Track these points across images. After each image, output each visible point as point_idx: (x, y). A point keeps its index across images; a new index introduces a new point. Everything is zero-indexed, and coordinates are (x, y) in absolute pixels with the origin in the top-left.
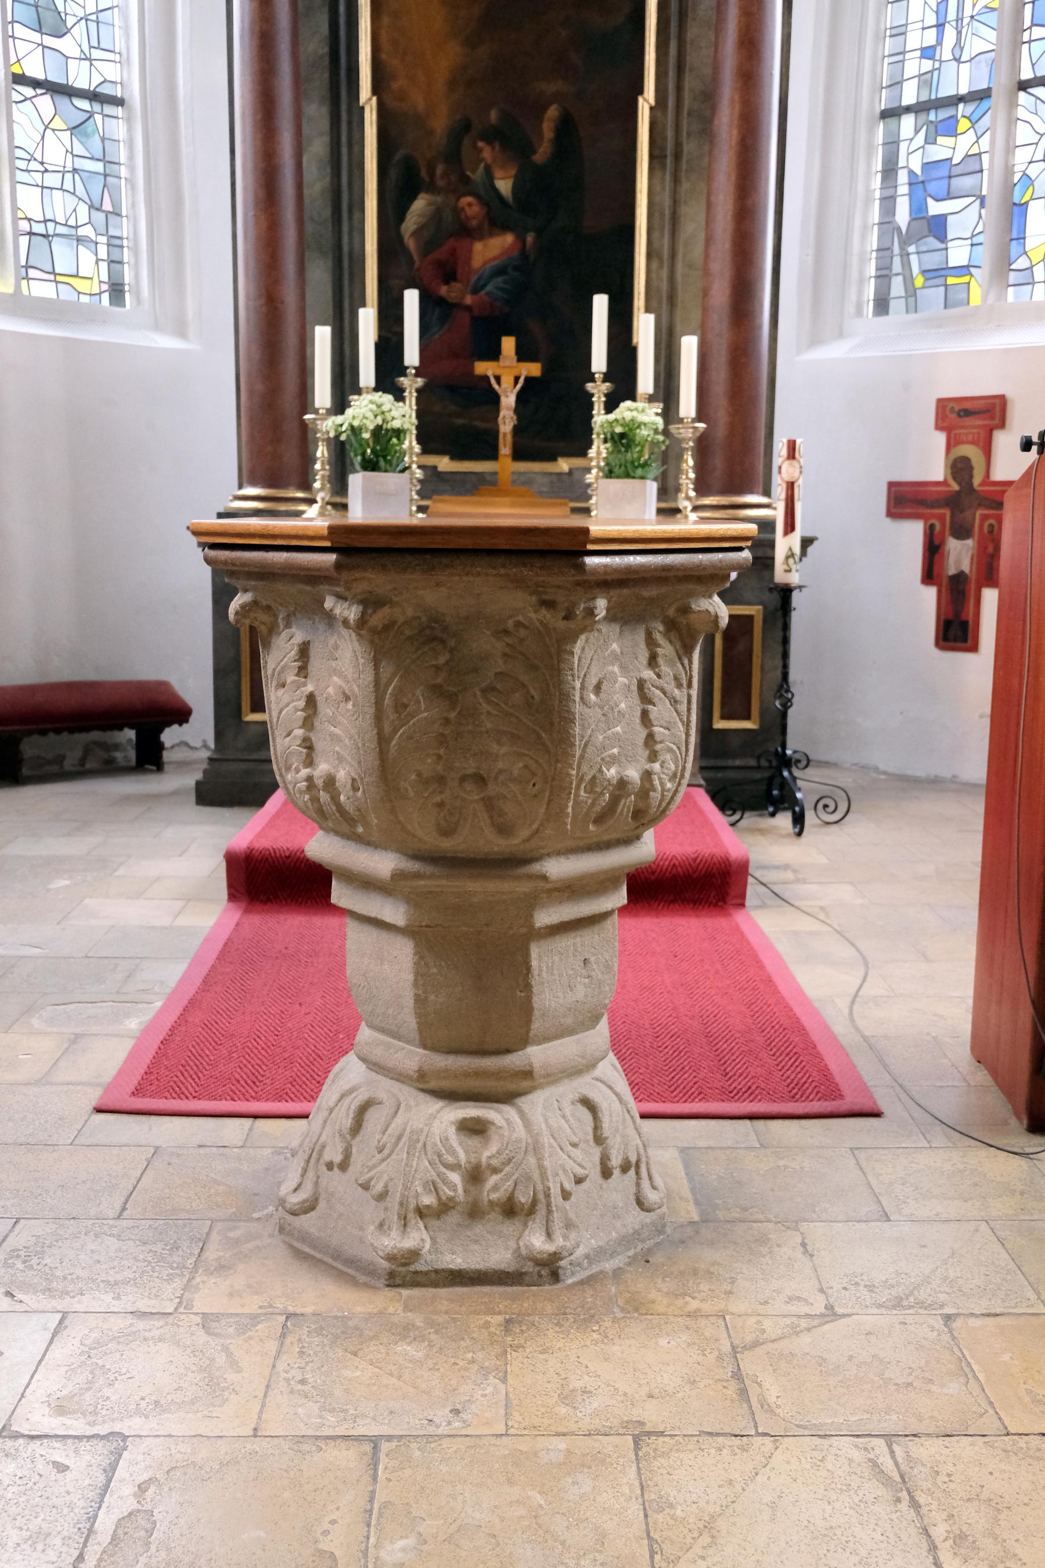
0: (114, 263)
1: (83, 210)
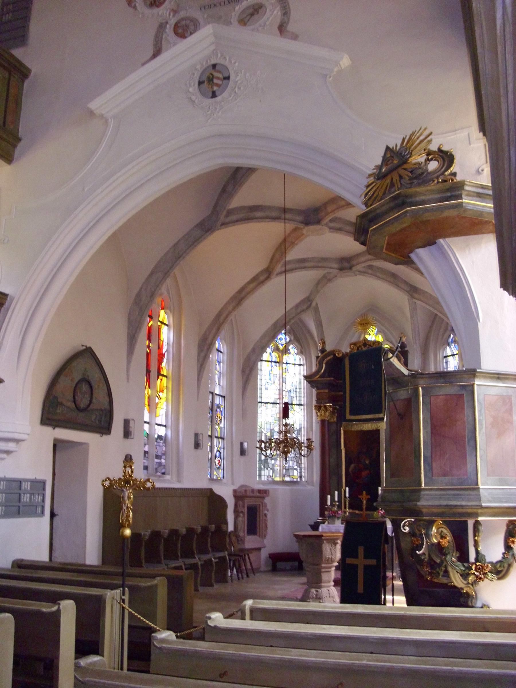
0: (301, 472)
1: (295, 463)
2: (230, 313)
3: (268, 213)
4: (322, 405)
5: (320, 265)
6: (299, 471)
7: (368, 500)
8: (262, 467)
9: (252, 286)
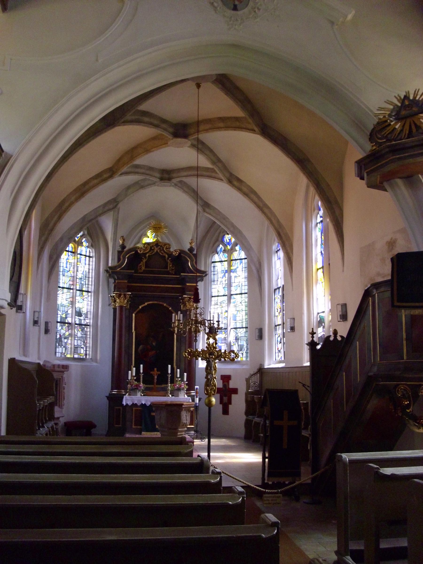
0: (86, 351)
1: (82, 343)
2: (72, 204)
3: (152, 120)
4: (122, 293)
5: (148, 172)
6: (85, 349)
7: (159, 376)
8: (57, 345)
9: (96, 181)
